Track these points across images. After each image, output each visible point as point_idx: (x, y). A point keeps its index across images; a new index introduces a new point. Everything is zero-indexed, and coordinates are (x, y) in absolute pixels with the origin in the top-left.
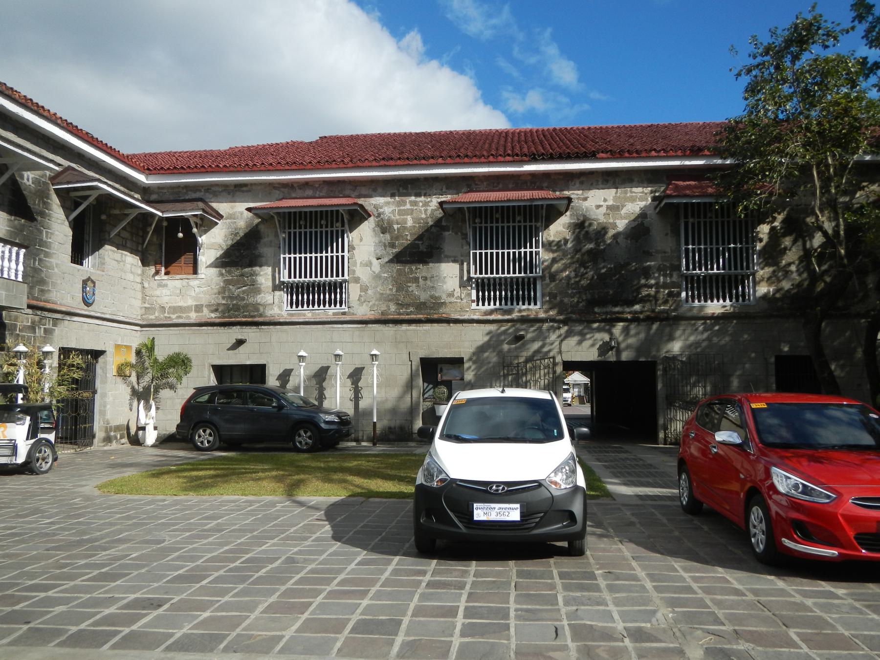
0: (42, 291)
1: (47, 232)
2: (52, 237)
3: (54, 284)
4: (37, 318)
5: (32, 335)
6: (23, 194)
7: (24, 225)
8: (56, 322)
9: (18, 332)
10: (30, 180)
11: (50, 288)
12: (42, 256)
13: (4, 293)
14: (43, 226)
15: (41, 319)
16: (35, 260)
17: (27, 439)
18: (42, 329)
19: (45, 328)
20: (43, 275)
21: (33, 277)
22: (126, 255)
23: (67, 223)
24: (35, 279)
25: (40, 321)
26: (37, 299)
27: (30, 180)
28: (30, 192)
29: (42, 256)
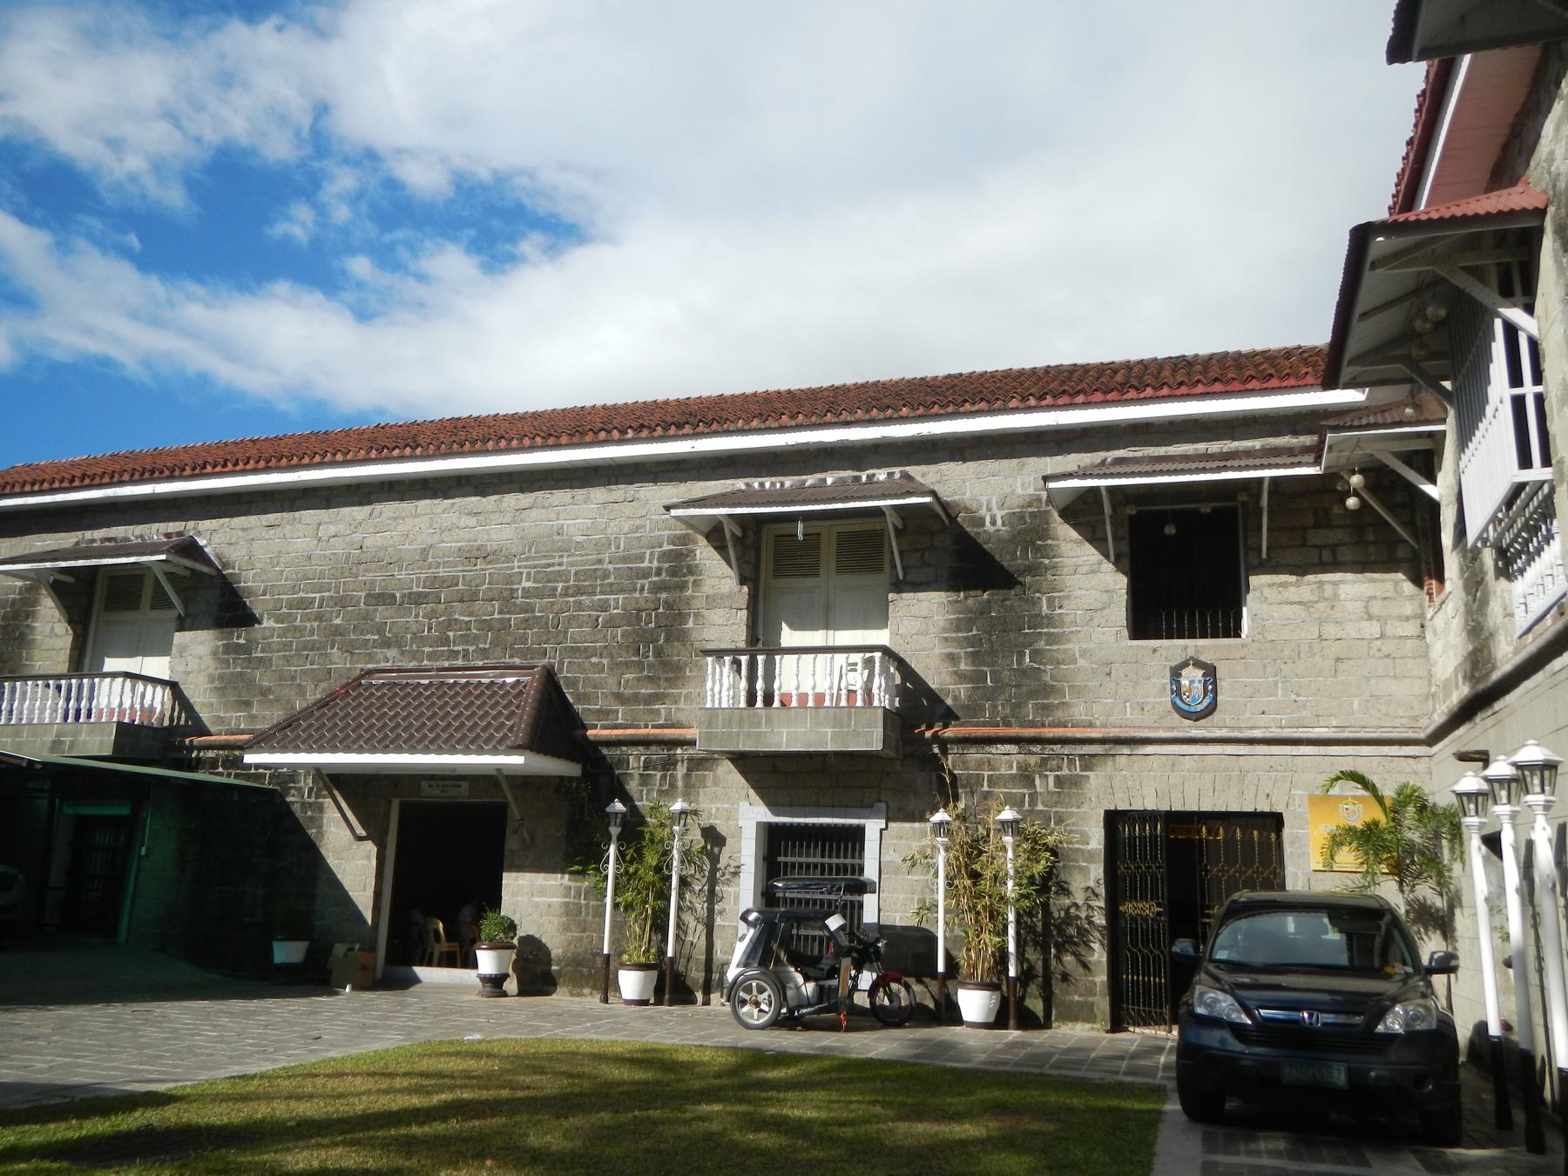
0: (1046, 708)
1: (1051, 601)
2: (1065, 603)
3: (1078, 691)
4: (1033, 760)
5: (1025, 791)
6: (985, 551)
7: (989, 601)
8: (1088, 762)
9: (986, 788)
10: (999, 522)
11: (1067, 699)
12: (1041, 644)
13: (829, 731)
14: (1038, 591)
15: (1043, 759)
16: (1021, 655)
17: (738, 966)
18: (1051, 780)
19: (1057, 777)
20: (1047, 678)
21: (1018, 686)
22: (1336, 584)
23: (1108, 567)
24: (1024, 689)
25: (1044, 762)
26: (1033, 724)
27: (999, 522)
28: (1000, 541)
29: (1041, 644)
